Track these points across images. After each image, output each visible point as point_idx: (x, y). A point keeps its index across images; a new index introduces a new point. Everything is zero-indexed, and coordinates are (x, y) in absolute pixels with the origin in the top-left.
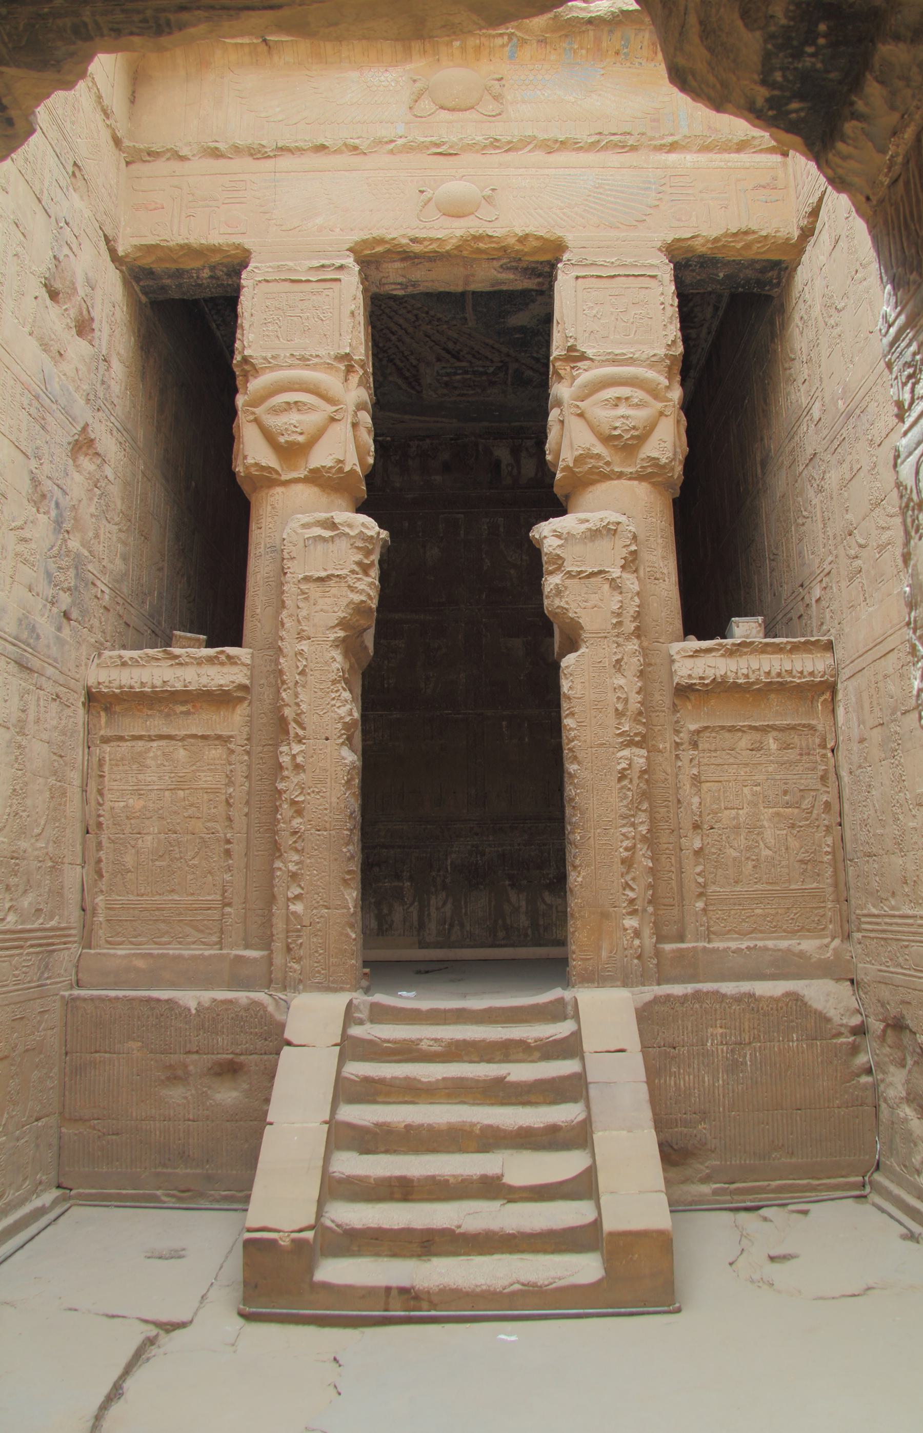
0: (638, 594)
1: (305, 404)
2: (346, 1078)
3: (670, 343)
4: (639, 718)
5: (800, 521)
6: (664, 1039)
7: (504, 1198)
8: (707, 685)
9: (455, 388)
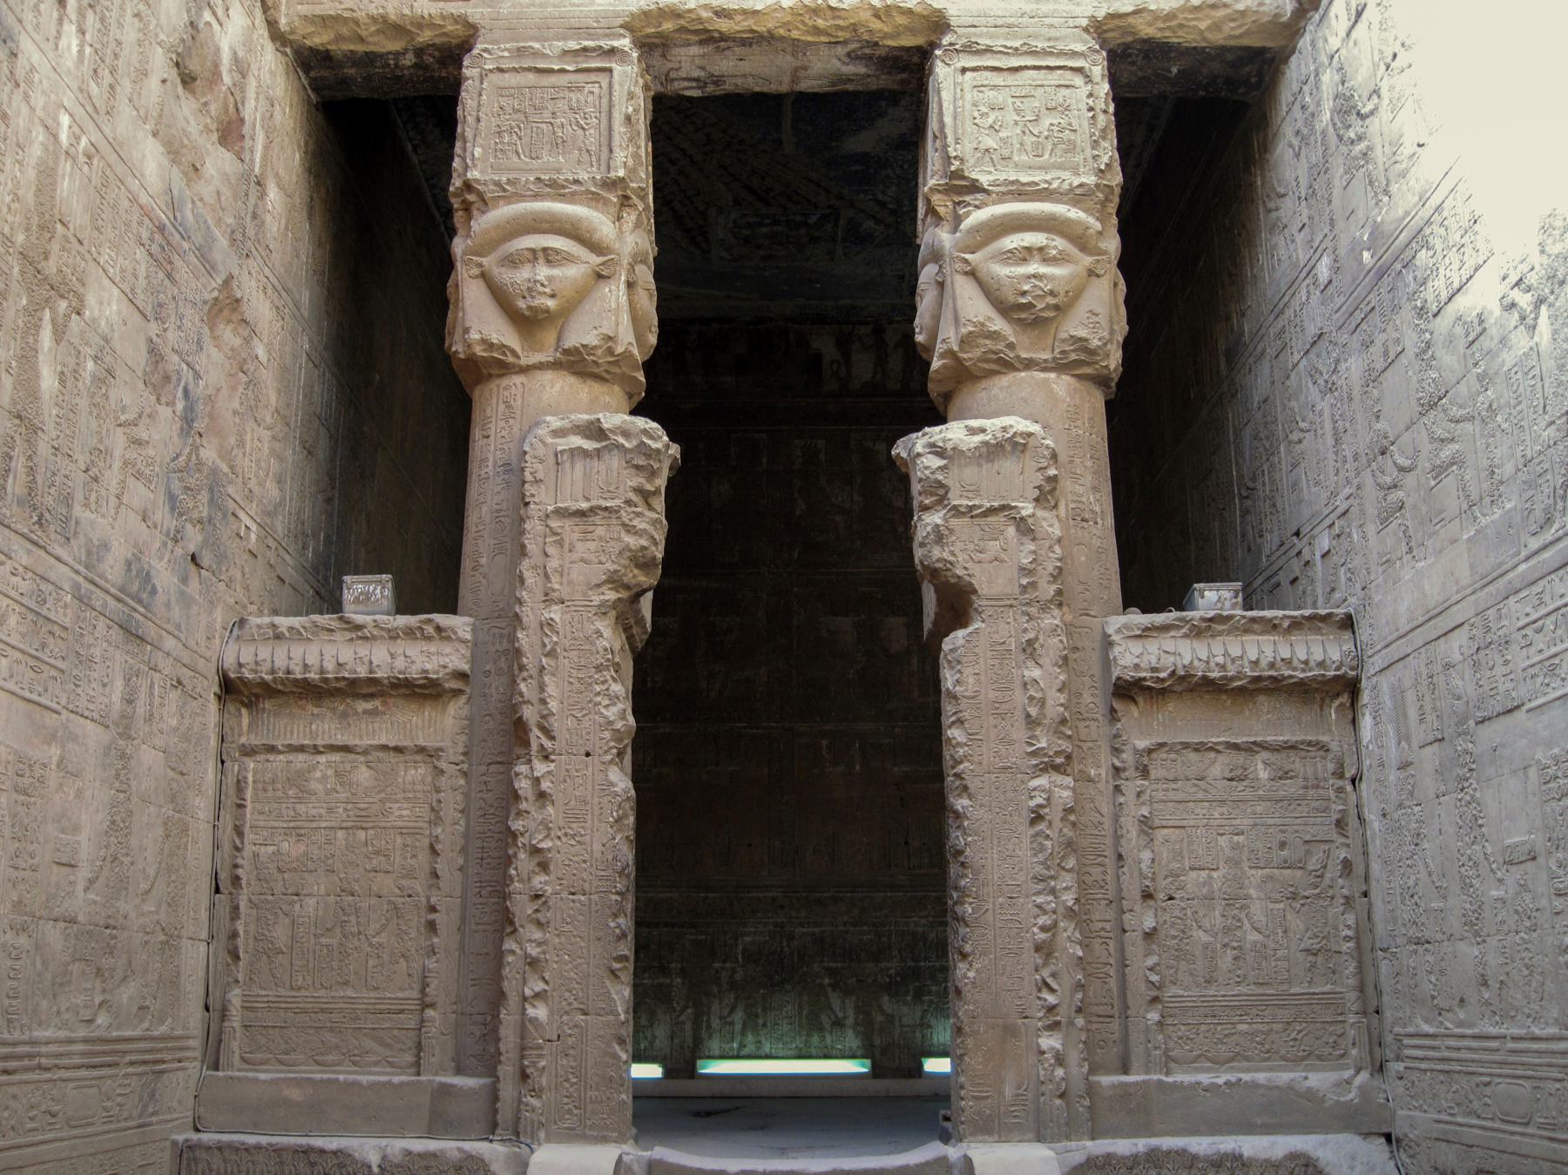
0: (1059, 541)
1: (557, 252)
3: (1103, 167)
5: (1295, 437)
8: (1163, 680)
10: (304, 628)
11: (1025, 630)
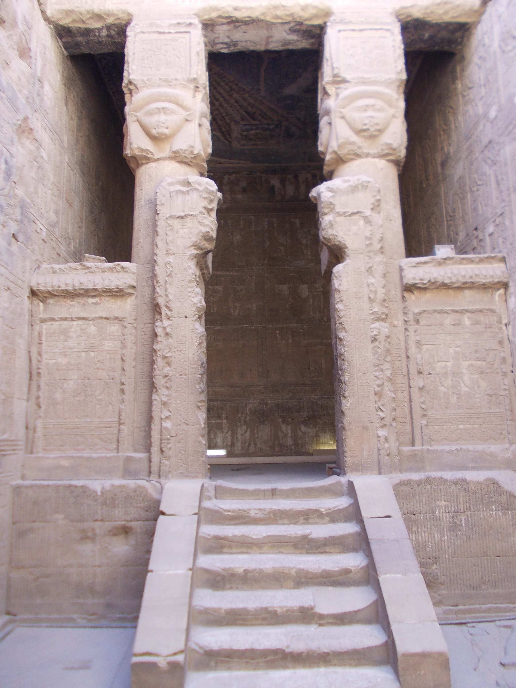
0: (382, 226)
1: (168, 109)
2: (202, 537)
4: (384, 303)
6: (407, 510)
7: (316, 623)
8: (425, 284)
9: (251, 140)
10: (65, 268)
11: (368, 263)
